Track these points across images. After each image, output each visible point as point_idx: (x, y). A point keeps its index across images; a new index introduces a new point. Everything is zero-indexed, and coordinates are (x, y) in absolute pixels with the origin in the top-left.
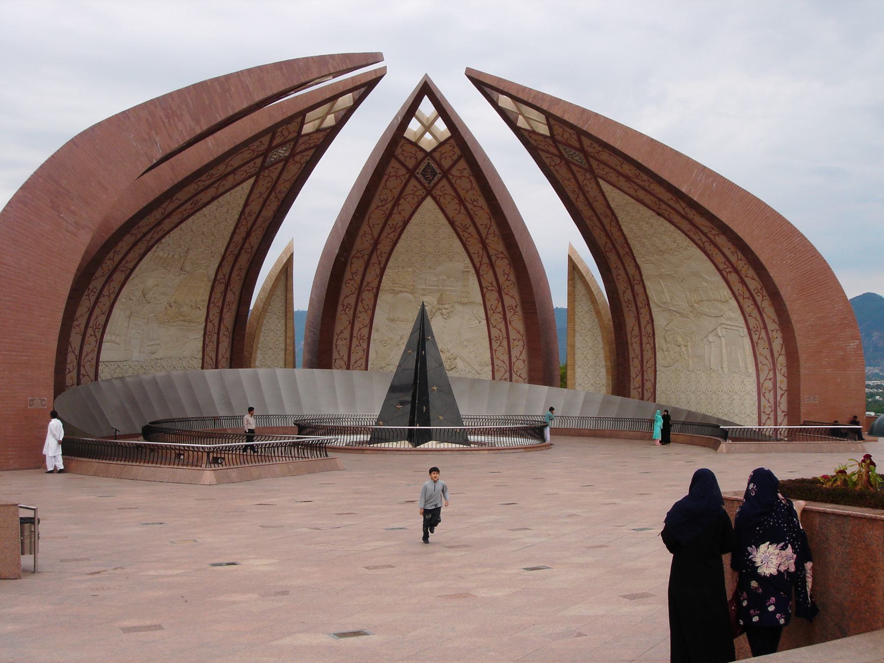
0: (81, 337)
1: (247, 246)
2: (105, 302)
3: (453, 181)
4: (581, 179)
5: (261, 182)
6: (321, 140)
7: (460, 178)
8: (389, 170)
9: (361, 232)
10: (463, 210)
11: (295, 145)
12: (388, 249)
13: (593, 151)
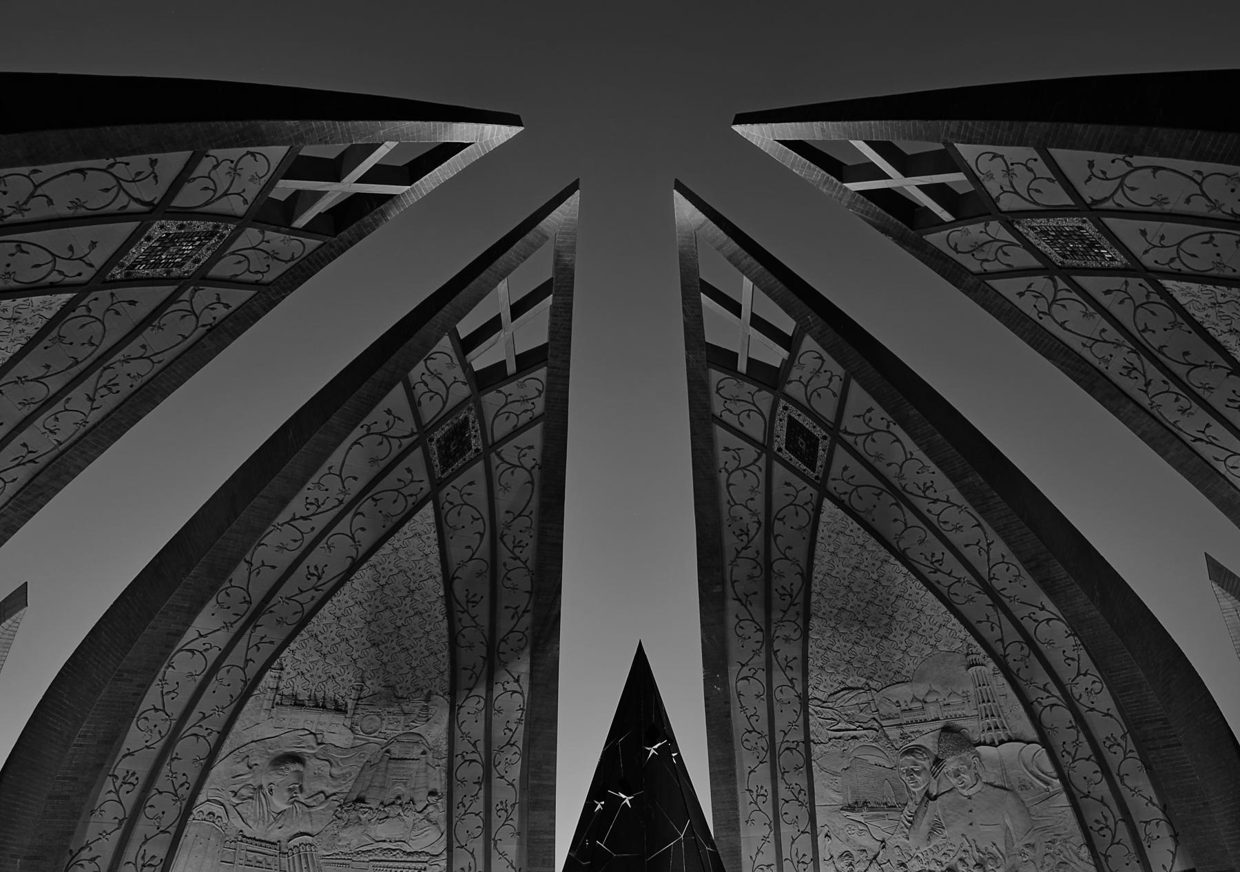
3: (859, 448)
4: (1123, 313)
5: (452, 518)
6: (539, 406)
7: (869, 434)
8: (723, 457)
9: (731, 621)
10: (912, 519)
11: (480, 416)
12: (794, 651)
13: (1108, 187)
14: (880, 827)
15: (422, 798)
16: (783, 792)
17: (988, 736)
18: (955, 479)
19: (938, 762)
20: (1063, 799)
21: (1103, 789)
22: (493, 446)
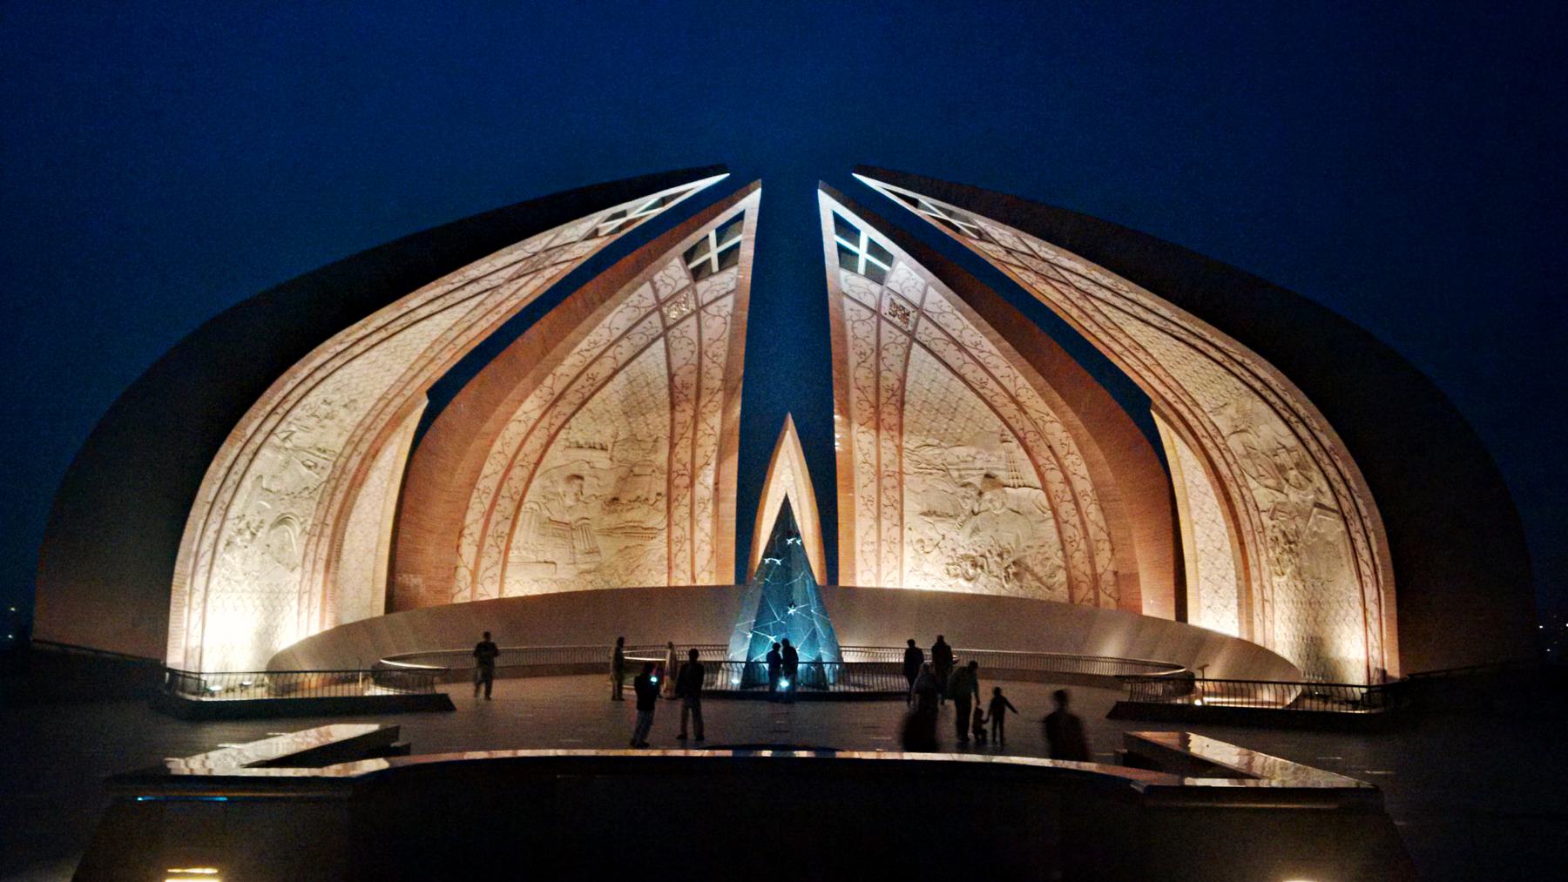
0: (475, 549)
1: (702, 426)
2: (506, 506)
8: (848, 314)
10: (967, 359)
12: (894, 420)
14: (943, 527)
15: (653, 497)
16: (884, 501)
17: (1011, 482)
18: (993, 342)
19: (980, 494)
20: (1052, 522)
21: (1075, 520)
22: (700, 308)
